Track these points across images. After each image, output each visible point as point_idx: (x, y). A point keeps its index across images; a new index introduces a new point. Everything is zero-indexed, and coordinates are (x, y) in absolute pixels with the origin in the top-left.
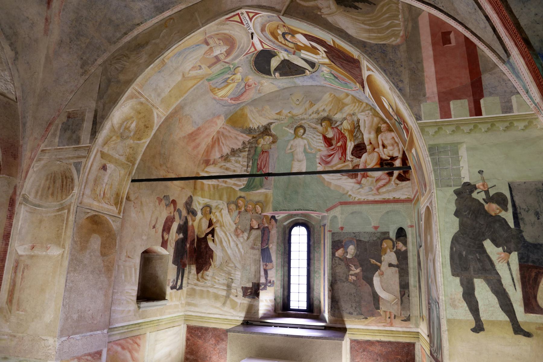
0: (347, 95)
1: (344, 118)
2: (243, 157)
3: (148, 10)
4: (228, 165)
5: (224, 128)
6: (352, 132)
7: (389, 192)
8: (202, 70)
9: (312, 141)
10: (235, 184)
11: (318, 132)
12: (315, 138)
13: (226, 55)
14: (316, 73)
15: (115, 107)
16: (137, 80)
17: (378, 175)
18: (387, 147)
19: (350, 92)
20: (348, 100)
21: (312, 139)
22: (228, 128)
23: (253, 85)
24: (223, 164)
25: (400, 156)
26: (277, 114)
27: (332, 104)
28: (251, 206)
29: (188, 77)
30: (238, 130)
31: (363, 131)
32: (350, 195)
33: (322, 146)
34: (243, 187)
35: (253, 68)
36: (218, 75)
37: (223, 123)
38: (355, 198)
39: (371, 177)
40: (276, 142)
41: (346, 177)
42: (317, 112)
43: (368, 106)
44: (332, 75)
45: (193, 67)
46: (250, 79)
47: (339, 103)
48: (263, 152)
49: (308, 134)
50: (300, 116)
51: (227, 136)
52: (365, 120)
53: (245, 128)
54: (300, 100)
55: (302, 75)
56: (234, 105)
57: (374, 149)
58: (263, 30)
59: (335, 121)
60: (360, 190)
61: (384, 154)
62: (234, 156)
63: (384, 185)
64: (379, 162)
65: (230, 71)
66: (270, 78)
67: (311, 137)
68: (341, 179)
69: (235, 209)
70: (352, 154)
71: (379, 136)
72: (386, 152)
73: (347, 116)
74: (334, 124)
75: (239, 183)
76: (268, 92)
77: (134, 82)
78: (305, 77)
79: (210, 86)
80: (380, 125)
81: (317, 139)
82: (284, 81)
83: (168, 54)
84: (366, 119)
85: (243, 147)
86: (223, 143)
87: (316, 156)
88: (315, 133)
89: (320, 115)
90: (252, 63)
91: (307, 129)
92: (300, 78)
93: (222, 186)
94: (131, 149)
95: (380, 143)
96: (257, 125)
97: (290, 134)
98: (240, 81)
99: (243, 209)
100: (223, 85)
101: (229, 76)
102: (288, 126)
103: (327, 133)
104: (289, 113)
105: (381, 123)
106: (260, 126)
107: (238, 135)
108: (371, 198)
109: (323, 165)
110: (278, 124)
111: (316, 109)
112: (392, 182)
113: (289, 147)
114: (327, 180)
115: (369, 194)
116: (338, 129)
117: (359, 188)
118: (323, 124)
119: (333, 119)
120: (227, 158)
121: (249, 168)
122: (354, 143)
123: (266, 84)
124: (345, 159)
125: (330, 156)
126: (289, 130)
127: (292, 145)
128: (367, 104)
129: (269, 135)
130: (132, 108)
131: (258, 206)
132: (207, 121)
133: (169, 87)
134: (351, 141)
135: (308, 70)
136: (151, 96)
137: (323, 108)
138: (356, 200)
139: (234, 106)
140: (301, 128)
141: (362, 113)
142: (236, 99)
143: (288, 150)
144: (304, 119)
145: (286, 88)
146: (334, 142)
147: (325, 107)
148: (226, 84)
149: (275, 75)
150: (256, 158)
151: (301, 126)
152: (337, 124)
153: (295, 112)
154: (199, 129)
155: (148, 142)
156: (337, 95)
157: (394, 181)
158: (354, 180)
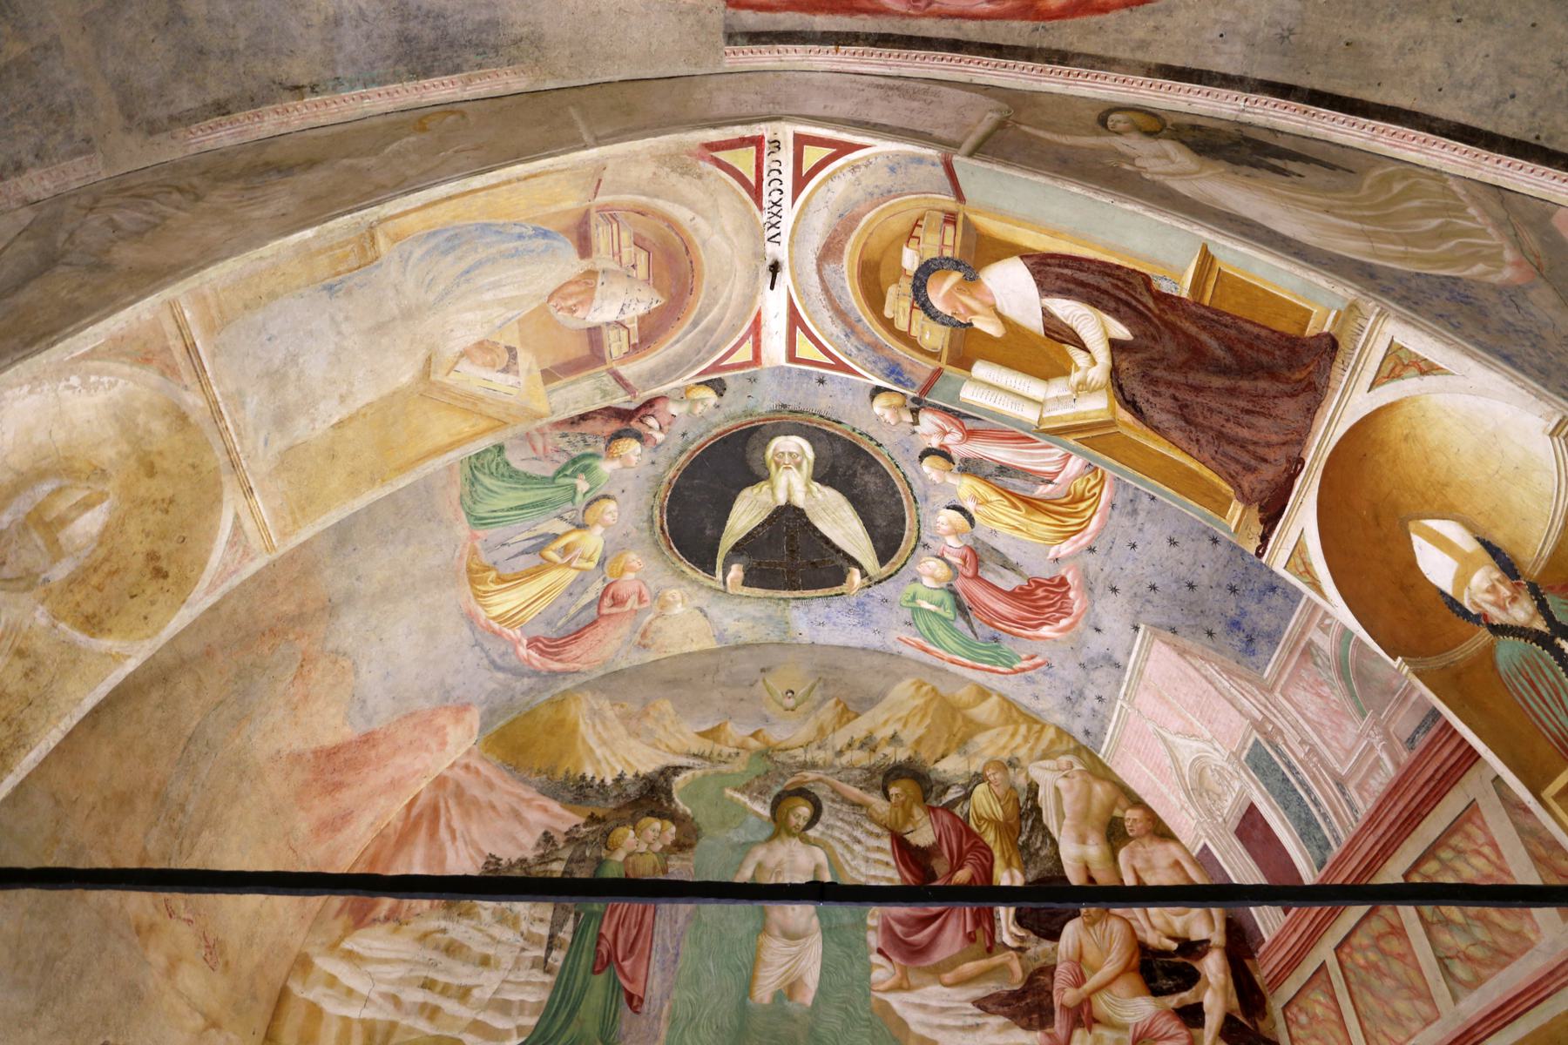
0: (983, 693)
1: (976, 774)
3: (368, 37)
5: (467, 767)
6: (1011, 827)
8: (511, 379)
9: (848, 857)
11: (871, 819)
12: (859, 842)
13: (635, 340)
14: (888, 586)
15: (24, 357)
16: (212, 273)
19: (993, 681)
20: (985, 711)
23: (632, 603)
25: (1218, 938)
26: (703, 735)
27: (928, 721)
29: (444, 389)
30: (530, 784)
31: (1053, 829)
35: (657, 519)
36: (521, 507)
37: (470, 744)
39: (1110, 1024)
40: (691, 846)
41: (1001, 1020)
42: (868, 744)
43: (1065, 738)
44: (948, 601)
45: (480, 345)
46: (632, 569)
47: (954, 718)
49: (828, 827)
51: (475, 802)
52: (1057, 789)
53: (560, 774)
54: (800, 692)
55: (827, 591)
56: (536, 673)
58: (830, 251)
59: (938, 782)
61: (1153, 927)
64: (1135, 961)
65: (569, 505)
66: (701, 586)
67: (845, 838)
68: (978, 1026)
71: (1123, 855)
72: (1157, 921)
73: (986, 767)
76: (675, 651)
77: (183, 278)
78: (837, 604)
79: (474, 552)
80: (1117, 813)
81: (868, 849)
82: (750, 609)
83: (406, 213)
84: (1062, 783)
85: (543, 856)
87: (863, 921)
88: (858, 824)
90: (665, 492)
91: (826, 805)
92: (814, 603)
94: (20, 666)
96: (613, 769)
97: (752, 819)
98: (592, 565)
100: (523, 563)
101: (559, 527)
102: (748, 785)
103: (909, 828)
104: (754, 735)
105: (1123, 802)
106: (629, 776)
107: (529, 802)
109: (896, 959)
110: (704, 776)
114: (916, 1028)
116: (953, 815)
118: (893, 790)
119: (933, 776)
122: (1024, 874)
123: (678, 609)
126: (749, 803)
128: (1060, 731)
129: (661, 816)
130: (124, 419)
132: (412, 714)
133: (342, 399)
134: (1009, 865)
135: (861, 567)
136: (243, 405)
137: (891, 733)
139: (534, 680)
140: (801, 801)
141: (1047, 763)
142: (549, 646)
144: (814, 766)
145: (746, 646)
146: (941, 866)
147: (898, 727)
148: (534, 560)
149: (725, 575)
151: (802, 793)
152: (952, 795)
153: (778, 734)
154: (368, 740)
155: (131, 666)
156: (944, 690)
158: (1039, 1034)
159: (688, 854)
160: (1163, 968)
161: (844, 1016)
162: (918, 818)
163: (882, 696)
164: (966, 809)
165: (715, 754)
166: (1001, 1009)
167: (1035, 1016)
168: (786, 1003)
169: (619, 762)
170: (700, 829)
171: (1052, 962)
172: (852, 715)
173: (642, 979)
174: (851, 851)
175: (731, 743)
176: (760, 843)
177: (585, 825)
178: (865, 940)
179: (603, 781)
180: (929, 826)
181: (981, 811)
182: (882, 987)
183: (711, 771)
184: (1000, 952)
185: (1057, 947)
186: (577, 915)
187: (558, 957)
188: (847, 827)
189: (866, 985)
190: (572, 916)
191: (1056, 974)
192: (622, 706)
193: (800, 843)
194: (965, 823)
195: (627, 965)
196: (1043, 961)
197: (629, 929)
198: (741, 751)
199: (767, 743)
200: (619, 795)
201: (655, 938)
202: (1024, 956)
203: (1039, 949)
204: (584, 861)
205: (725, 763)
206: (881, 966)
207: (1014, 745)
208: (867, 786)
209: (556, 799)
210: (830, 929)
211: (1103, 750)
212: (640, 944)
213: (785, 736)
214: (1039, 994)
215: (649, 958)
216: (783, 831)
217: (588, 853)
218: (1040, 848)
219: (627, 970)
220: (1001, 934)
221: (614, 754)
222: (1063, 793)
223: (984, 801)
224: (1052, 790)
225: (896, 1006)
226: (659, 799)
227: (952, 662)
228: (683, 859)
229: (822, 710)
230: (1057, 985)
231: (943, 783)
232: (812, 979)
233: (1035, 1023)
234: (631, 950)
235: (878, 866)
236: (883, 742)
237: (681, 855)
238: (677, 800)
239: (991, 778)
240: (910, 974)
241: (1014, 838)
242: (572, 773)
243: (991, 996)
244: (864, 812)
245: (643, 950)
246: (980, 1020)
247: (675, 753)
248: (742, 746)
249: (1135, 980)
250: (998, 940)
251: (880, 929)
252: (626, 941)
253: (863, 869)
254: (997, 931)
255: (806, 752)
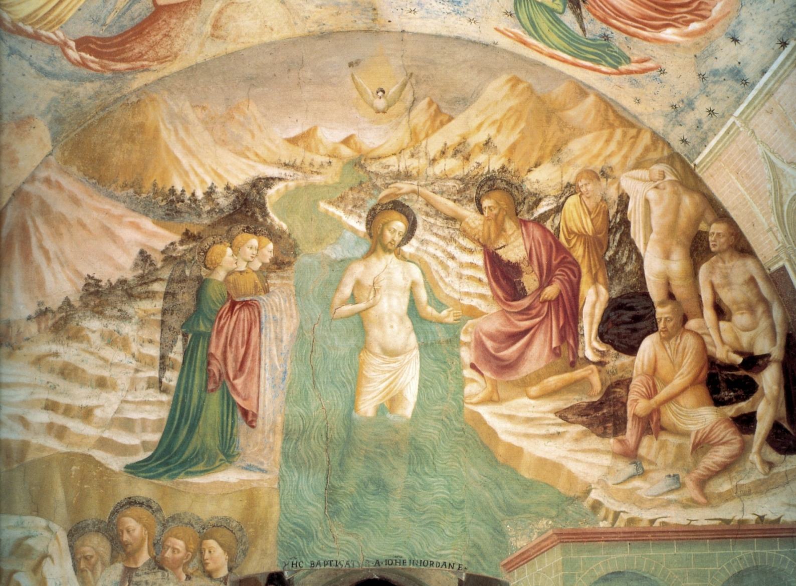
0: (582, 91)
1: (569, 185)
2: (143, 323)
4: (70, 353)
7: (740, 493)
10: (104, 444)
11: (465, 234)
12: (453, 258)
17: (699, 427)
18: (731, 314)
21: (441, 263)
22: (65, 181)
24: (44, 347)
26: (293, 141)
27: (523, 125)
28: (180, 544)
30: (117, 199)
31: (640, 244)
32: (596, 506)
33: (482, 296)
34: (142, 456)
38: (617, 515)
39: (676, 432)
40: (289, 264)
41: (580, 428)
42: (461, 151)
43: (660, 145)
48: (234, 304)
49: (423, 242)
50: (393, 160)
52: (647, 201)
54: (392, 90)
57: (685, 319)
60: (637, 483)
62: (98, 312)
63: (725, 468)
64: (704, 374)
67: (439, 254)
69: (107, 558)
70: (602, 336)
71: (703, 270)
72: (727, 337)
73: (579, 177)
74: (531, 209)
75: (125, 439)
76: (256, 41)
80: (703, 227)
85: (142, 277)
86: (46, 253)
88: (452, 239)
89: (472, 164)
91: (420, 219)
93: (42, 448)
95: (706, 296)
96: (203, 181)
97: (348, 234)
99: (144, 557)
102: (342, 198)
103: (502, 242)
104: (346, 142)
105: (709, 216)
106: (220, 189)
107: (119, 218)
108: (676, 517)
109: (487, 374)
111: (457, 139)
112: (754, 457)
113: (347, 291)
114: (504, 437)
115: (669, 502)
117: (632, 477)
118: (486, 203)
120: (66, 320)
121: (168, 374)
122: (609, 290)
124: (575, 355)
125: (515, 337)
127: (358, 284)
128: (656, 138)
131: (212, 543)
134: (595, 280)
138: (621, 524)
140: (395, 214)
143: (345, 303)
145: (331, 33)
146: (530, 281)
147: (492, 132)
150: (202, 328)
151: (398, 206)
152: (543, 208)
157: (759, 452)
158: (612, 440)
159: (289, 272)
160: (727, 381)
161: (440, 426)
162: (510, 232)
163: (477, 94)
164: (557, 222)
165: (307, 163)
166: (580, 419)
167: (610, 425)
168: (388, 415)
169: (207, 172)
170: (296, 246)
171: (627, 376)
172: (445, 118)
173: (254, 396)
174: (446, 267)
175: (322, 151)
176: (357, 259)
177: (182, 242)
178: (459, 356)
179: (193, 194)
180: (521, 240)
181: (571, 225)
182: (475, 400)
183: (303, 182)
184: (581, 367)
185: (633, 361)
186: (185, 335)
187: (172, 378)
188: (442, 243)
189: (459, 394)
190: (180, 337)
191: (631, 386)
192: (204, 108)
193: (395, 259)
194: (556, 236)
195: (239, 382)
196: (620, 374)
197: (237, 348)
198: (334, 160)
199: (359, 150)
200: (212, 210)
201: (263, 356)
202: (603, 369)
203: (618, 363)
204: (184, 281)
205: (318, 173)
206: (473, 380)
207: (608, 152)
208: (459, 196)
209: (147, 215)
210: (426, 345)
211: (697, 161)
212: (248, 364)
213: (377, 143)
214: (615, 405)
215: (259, 377)
216: (379, 247)
217: (187, 273)
218: (626, 263)
219: (239, 387)
220: (584, 349)
221: (202, 165)
222: (652, 205)
223: (575, 215)
224: (642, 202)
225: (487, 417)
226: (254, 214)
227: (552, 57)
228: (283, 278)
229: (414, 113)
230: (632, 396)
231: (535, 195)
232: (411, 394)
233: (609, 431)
234: (241, 368)
235: (470, 282)
236: (477, 150)
237: (281, 274)
238: (272, 214)
239: (583, 189)
240: (500, 388)
241: (601, 253)
242: (160, 186)
243: (572, 407)
244: (458, 226)
245: (252, 370)
246: (561, 429)
247: (265, 162)
248: (333, 154)
249: (702, 391)
250: (581, 355)
251: (472, 345)
252: (236, 361)
253: (457, 286)
254: (580, 346)
255: (399, 161)
